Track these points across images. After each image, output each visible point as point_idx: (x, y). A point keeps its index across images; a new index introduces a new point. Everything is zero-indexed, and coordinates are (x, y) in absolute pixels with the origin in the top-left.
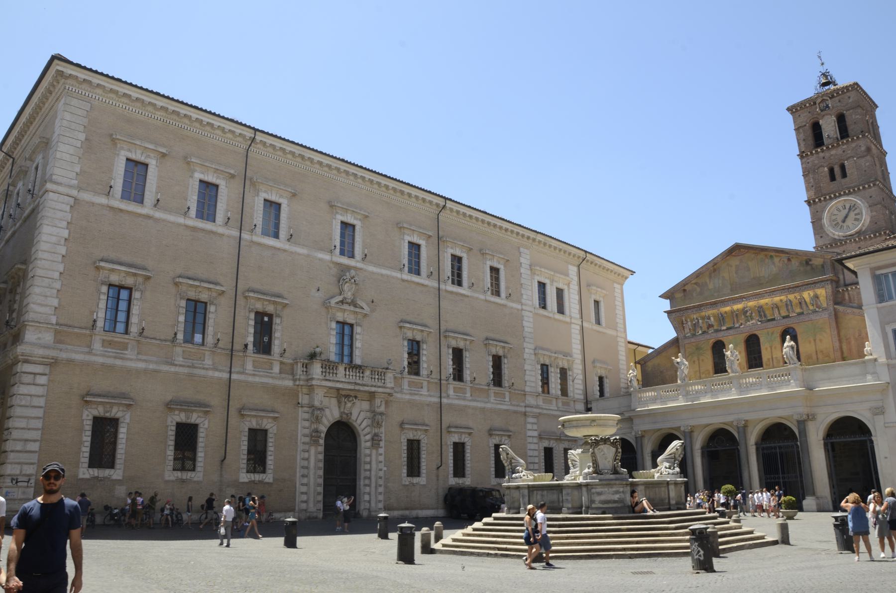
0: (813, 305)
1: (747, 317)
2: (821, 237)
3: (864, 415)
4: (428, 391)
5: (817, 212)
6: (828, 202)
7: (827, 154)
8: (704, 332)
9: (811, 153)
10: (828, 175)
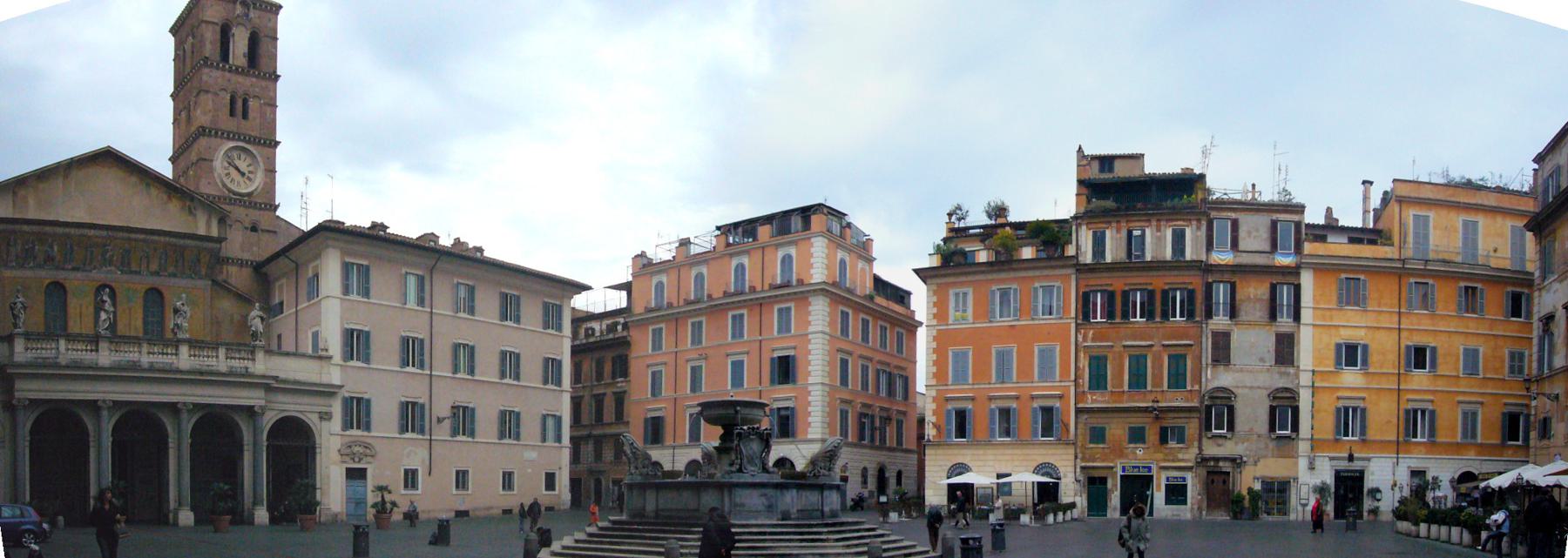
0: (190, 269)
2: (209, 183)
3: (312, 420)
5: (210, 148)
6: (224, 141)
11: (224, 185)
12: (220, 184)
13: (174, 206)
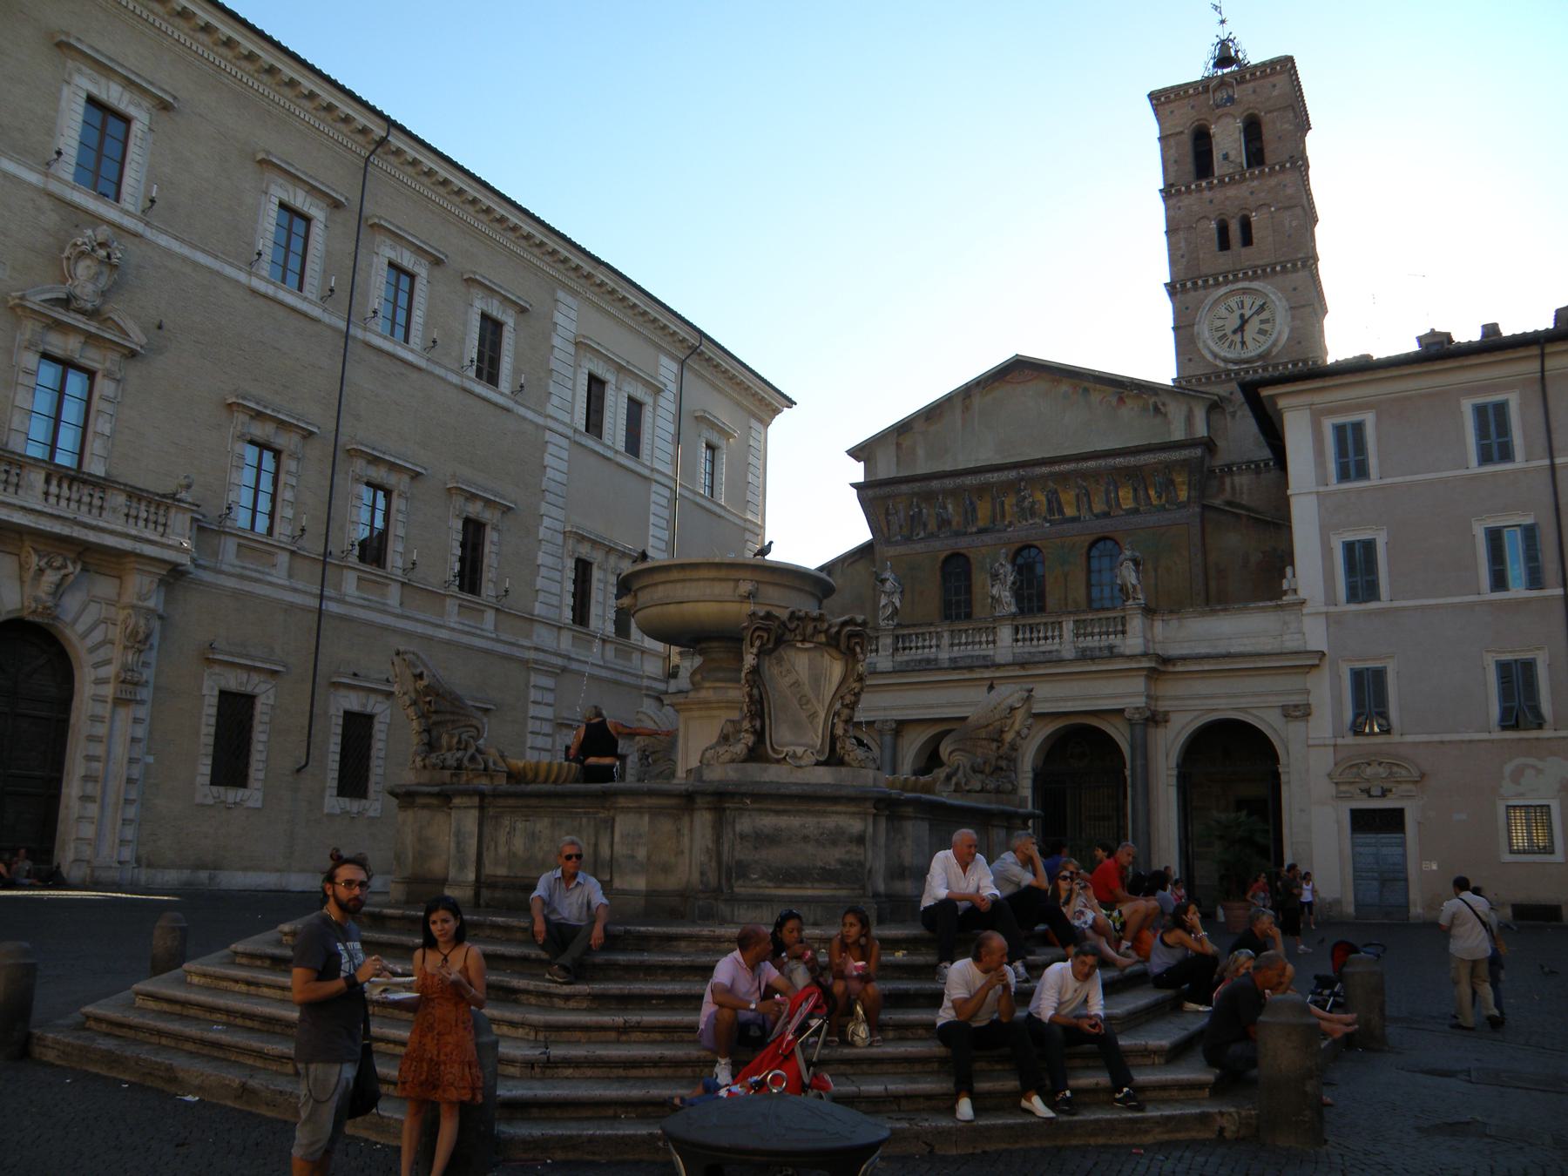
1: (1023, 509)
2: (1190, 360)
3: (1268, 721)
4: (290, 576)
5: (1187, 308)
6: (1211, 290)
7: (1218, 195)
8: (931, 536)
9: (1188, 187)
10: (1216, 236)
11: (1215, 356)
12: (1209, 357)
13: (1130, 410)
